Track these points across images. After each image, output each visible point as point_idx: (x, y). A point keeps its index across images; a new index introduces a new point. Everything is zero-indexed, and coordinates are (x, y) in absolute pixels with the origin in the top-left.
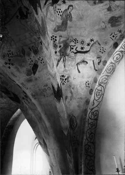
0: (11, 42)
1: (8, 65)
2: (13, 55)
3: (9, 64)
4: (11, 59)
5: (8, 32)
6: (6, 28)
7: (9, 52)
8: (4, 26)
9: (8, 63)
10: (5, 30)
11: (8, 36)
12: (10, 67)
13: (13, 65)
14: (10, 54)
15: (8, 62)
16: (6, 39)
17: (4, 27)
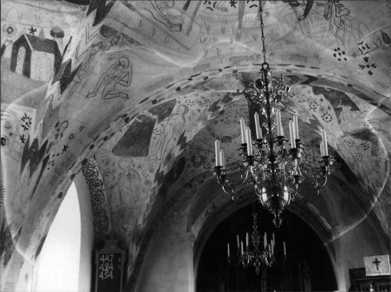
0: (359, 26)
1: (366, 70)
2: (369, 48)
3: (368, 66)
4: (368, 58)
5: (348, 10)
6: (342, 5)
7: (360, 47)
8: (337, 4)
9: (365, 65)
10: (342, 9)
11: (349, 18)
12: (372, 71)
13: (375, 67)
14: (364, 48)
15: (364, 64)
16: (348, 23)
17: (339, 5)
